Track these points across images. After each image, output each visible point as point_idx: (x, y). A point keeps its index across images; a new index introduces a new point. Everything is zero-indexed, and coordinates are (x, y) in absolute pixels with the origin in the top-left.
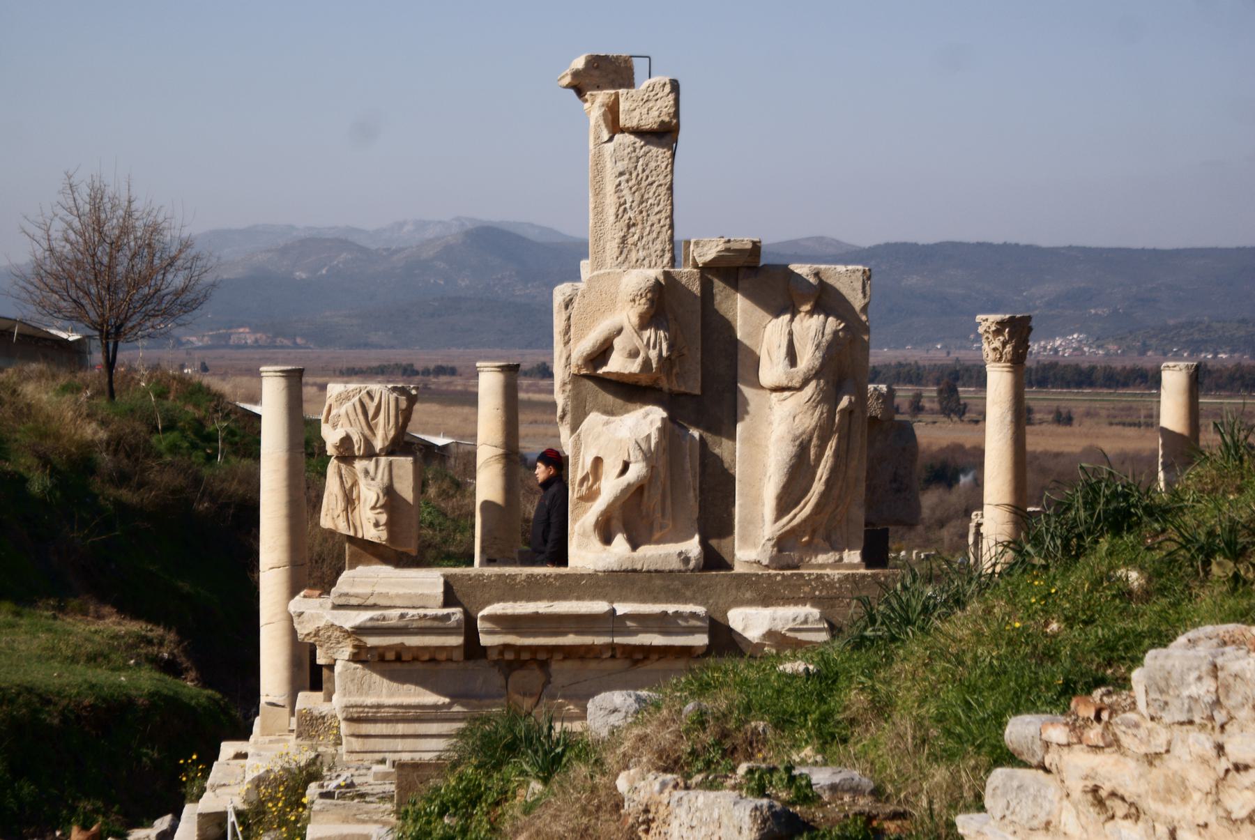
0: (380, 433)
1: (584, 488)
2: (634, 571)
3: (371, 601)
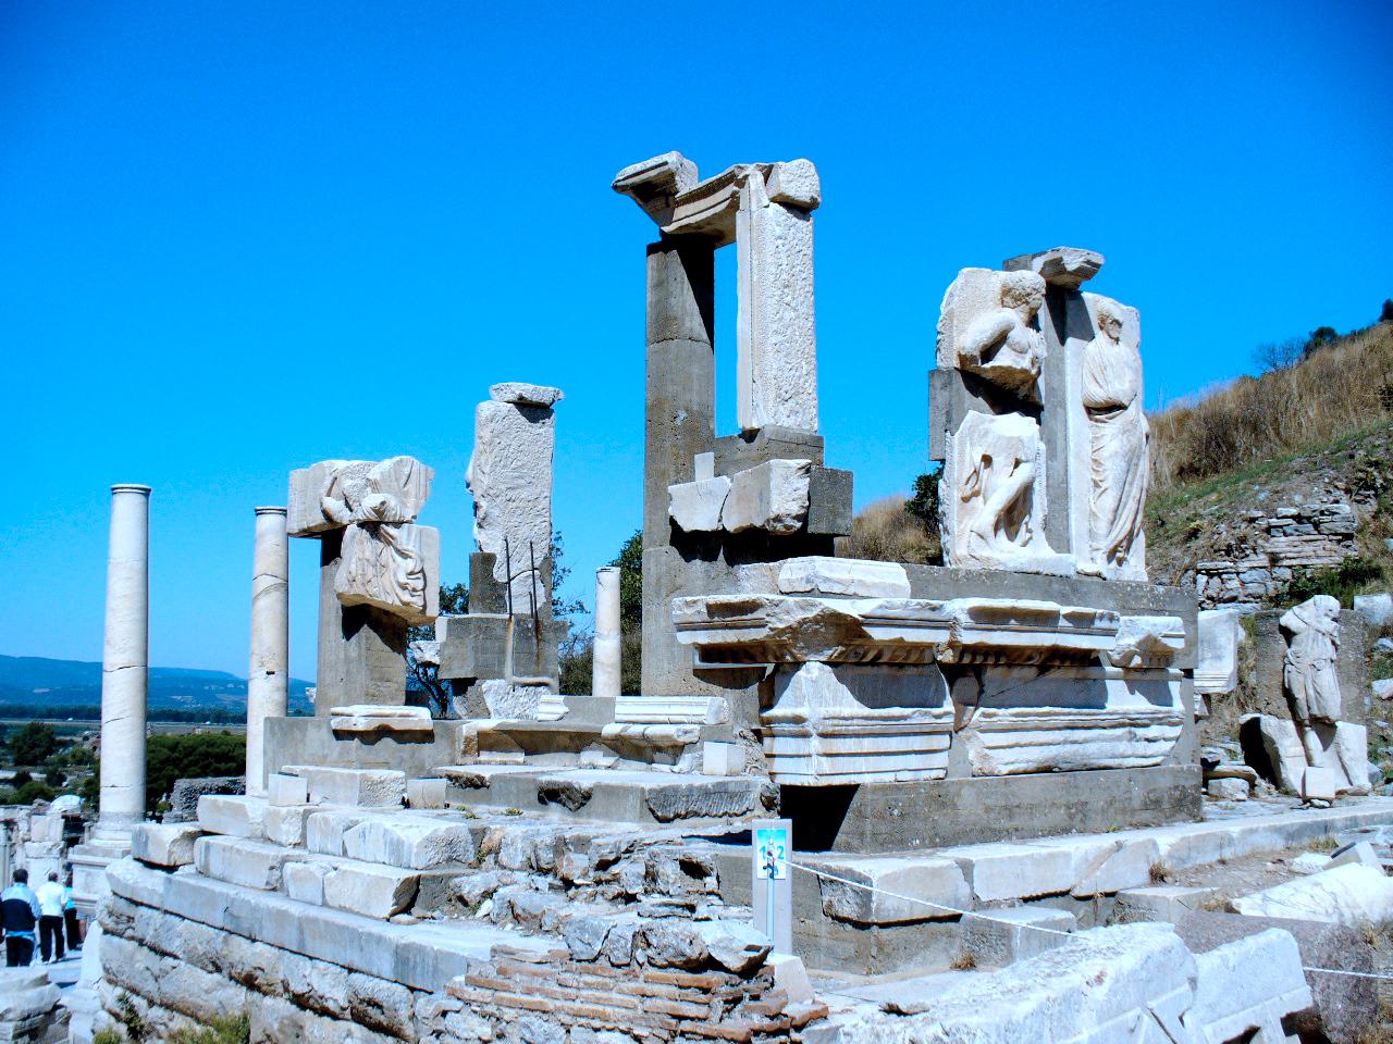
0: (412, 501)
1: (969, 486)
2: (1038, 573)
3: (850, 591)
